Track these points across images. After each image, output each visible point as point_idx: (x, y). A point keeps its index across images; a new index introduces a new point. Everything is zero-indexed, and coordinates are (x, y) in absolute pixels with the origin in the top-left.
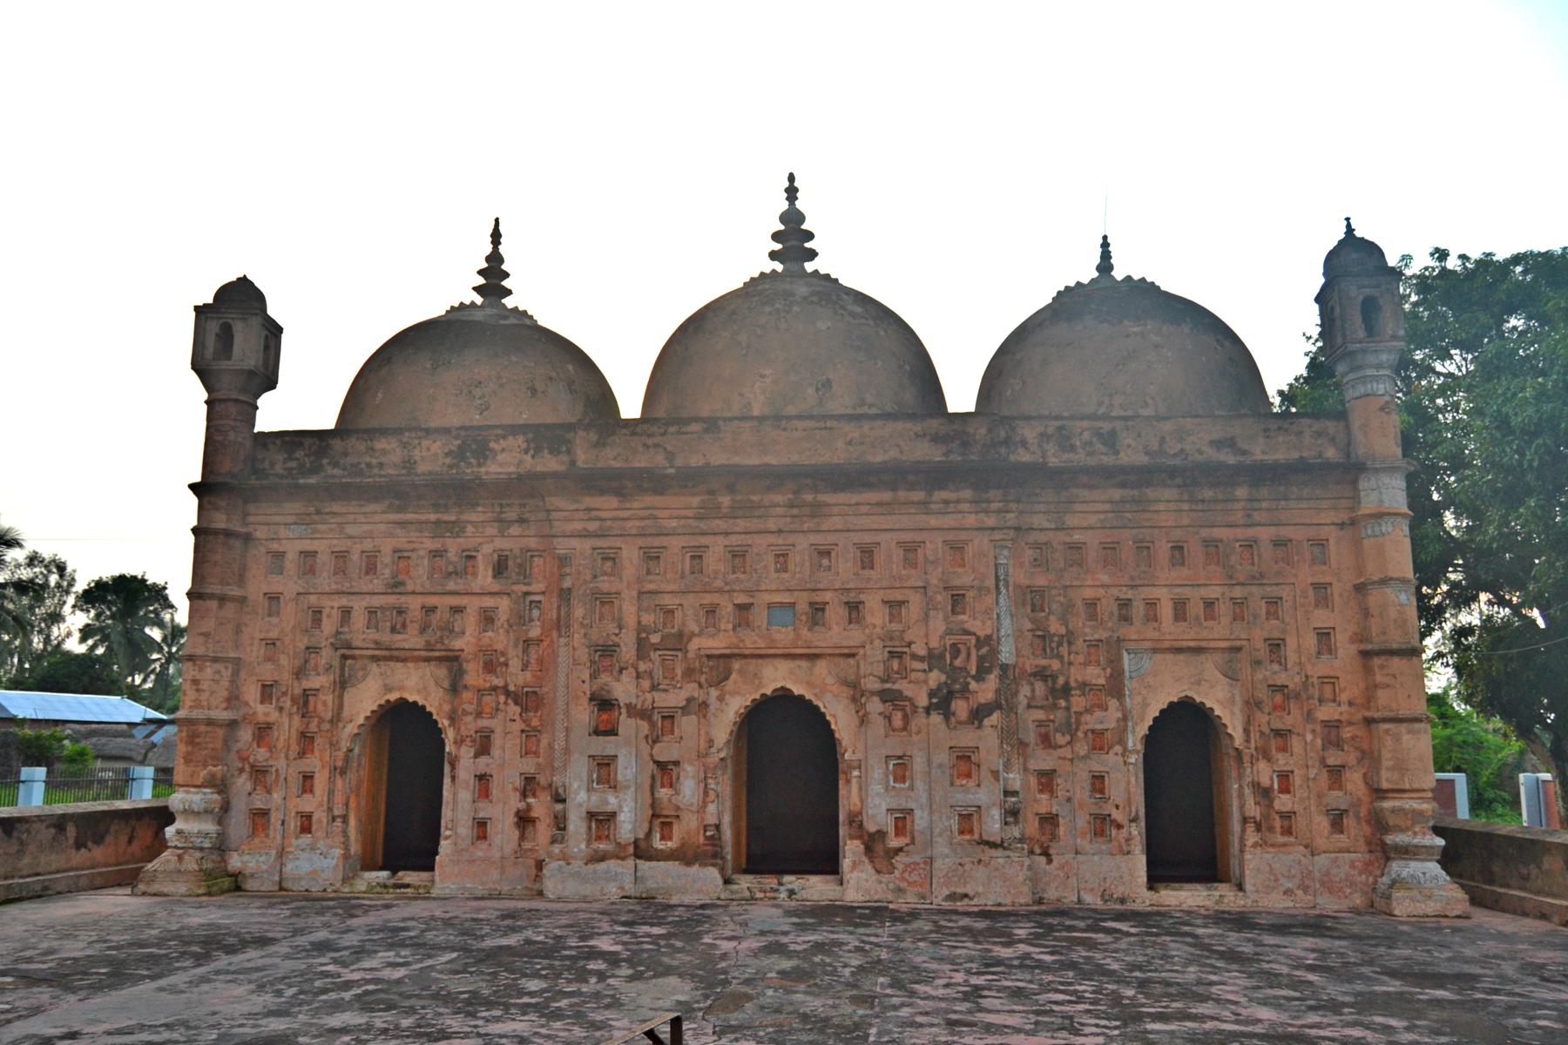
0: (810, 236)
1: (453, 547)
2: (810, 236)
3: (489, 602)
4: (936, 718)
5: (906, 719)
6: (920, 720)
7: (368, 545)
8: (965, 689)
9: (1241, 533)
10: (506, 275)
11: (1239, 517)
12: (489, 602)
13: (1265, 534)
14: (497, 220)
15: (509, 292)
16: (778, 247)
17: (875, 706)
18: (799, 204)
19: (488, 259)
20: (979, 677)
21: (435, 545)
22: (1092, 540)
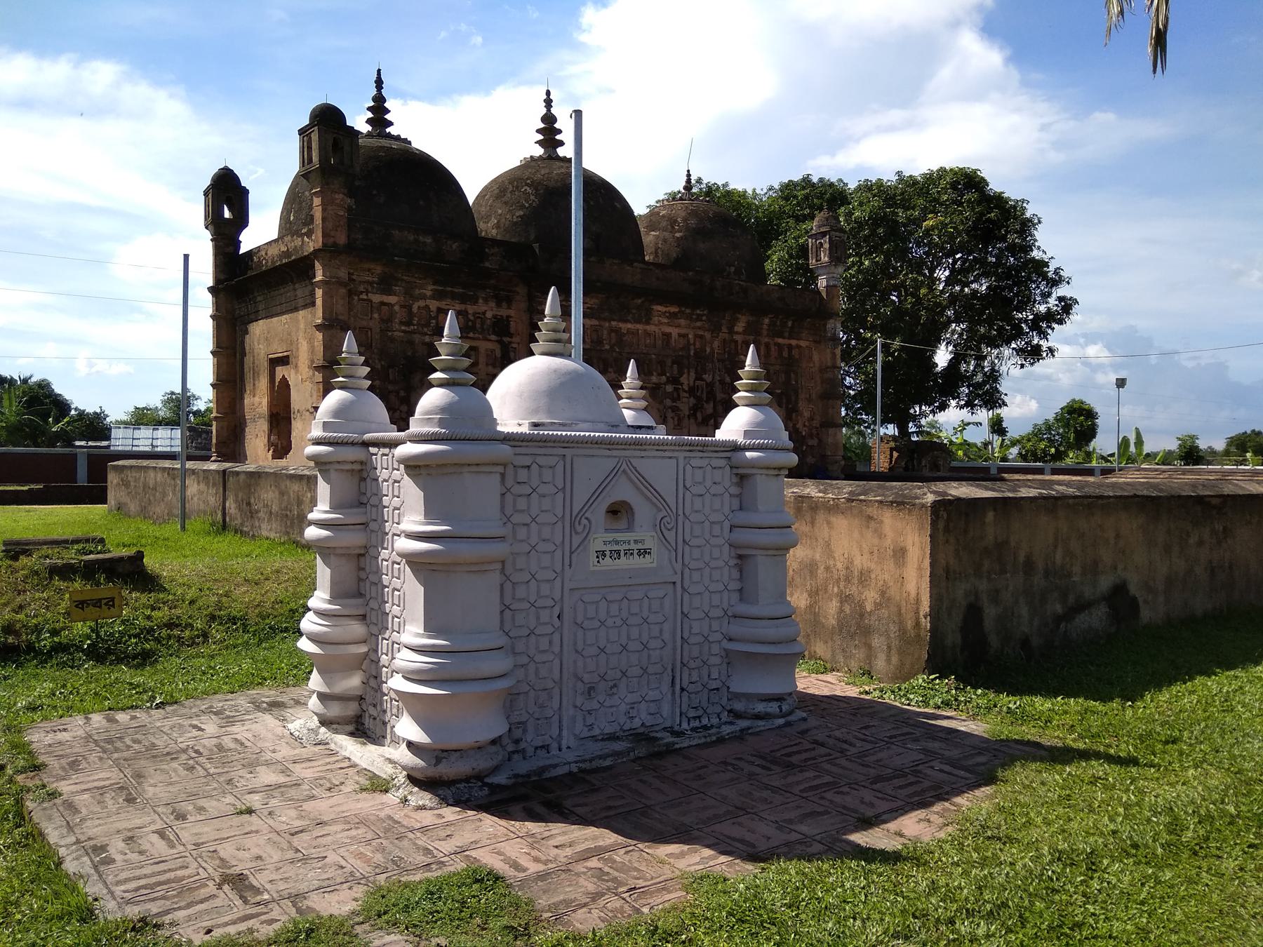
0: (560, 132)
1: (471, 309)
2: (560, 132)
3: (490, 346)
4: (692, 421)
5: (680, 420)
6: (686, 421)
7: (422, 303)
8: (702, 407)
9: (786, 341)
10: (388, 111)
11: (786, 334)
12: (490, 346)
13: (794, 342)
14: (379, 71)
15: (391, 124)
16: (541, 137)
17: (670, 414)
18: (553, 110)
19: (374, 99)
20: (707, 402)
21: (462, 307)
22: (738, 338)
